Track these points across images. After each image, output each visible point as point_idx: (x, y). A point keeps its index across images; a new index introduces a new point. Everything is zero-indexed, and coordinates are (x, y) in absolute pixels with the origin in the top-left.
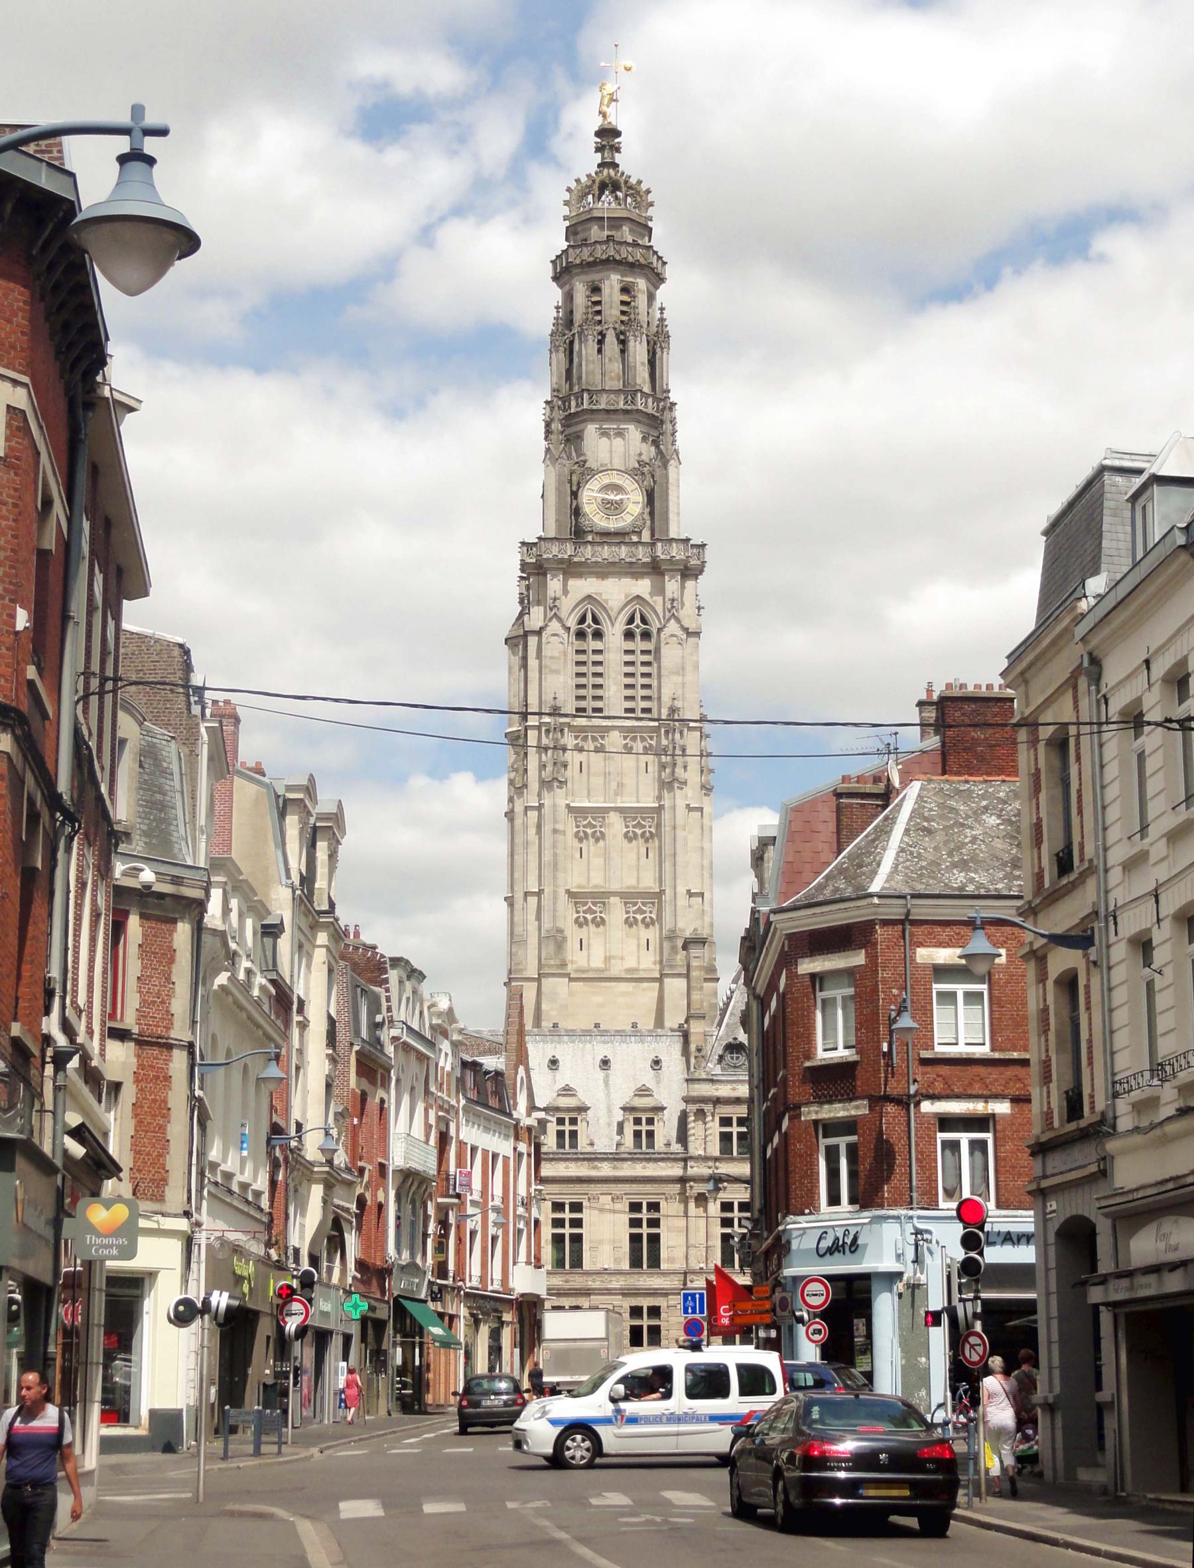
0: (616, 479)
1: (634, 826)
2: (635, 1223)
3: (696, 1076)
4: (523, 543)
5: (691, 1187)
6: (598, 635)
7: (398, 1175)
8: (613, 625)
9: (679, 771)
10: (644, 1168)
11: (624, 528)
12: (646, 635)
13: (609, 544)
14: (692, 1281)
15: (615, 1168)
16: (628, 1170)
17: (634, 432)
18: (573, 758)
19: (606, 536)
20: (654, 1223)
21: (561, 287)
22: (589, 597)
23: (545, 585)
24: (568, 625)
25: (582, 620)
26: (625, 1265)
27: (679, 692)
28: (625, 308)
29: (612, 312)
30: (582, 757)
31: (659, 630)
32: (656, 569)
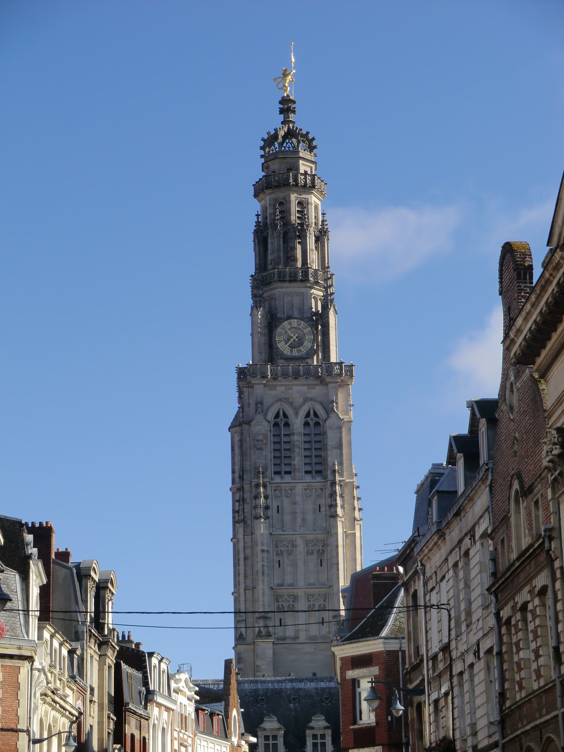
1: (312, 546)
6: (287, 424)
12: (317, 424)
21: (260, 201)
25: (277, 416)
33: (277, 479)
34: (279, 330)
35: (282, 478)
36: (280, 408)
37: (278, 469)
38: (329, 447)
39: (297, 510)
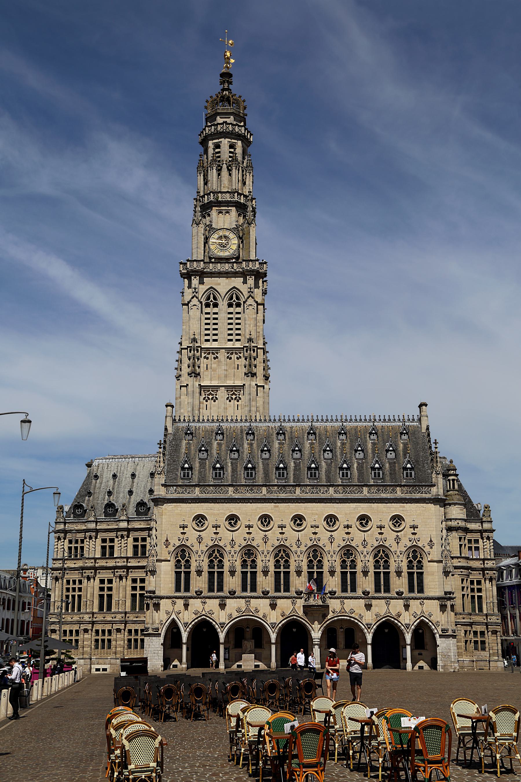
0: (227, 233)
6: (216, 305)
11: (228, 256)
13: (220, 263)
18: (203, 362)
19: (220, 260)
24: (202, 300)
25: (208, 298)
28: (231, 155)
31: (244, 302)
36: (210, 294)
37: (207, 338)
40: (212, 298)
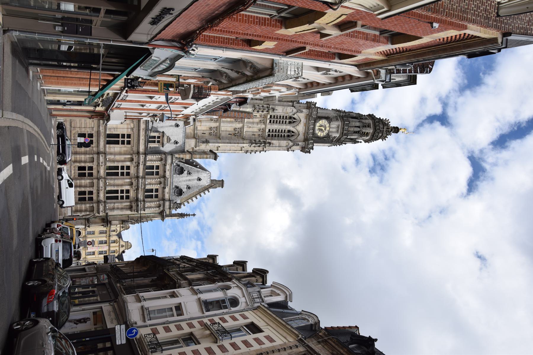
1: (238, 131)
2: (123, 136)
3: (174, 158)
4: (316, 103)
5: (136, 156)
6: (290, 123)
7: (268, 64)
8: (293, 127)
9: (254, 145)
10: (143, 139)
14: (102, 156)
15: (143, 129)
16: (142, 133)
17: (337, 135)
20: (123, 142)
22: (301, 121)
23: (304, 109)
24: (295, 115)
25: (294, 119)
26: (108, 132)
27: (274, 145)
29: (365, 130)
30: (258, 116)
31: (291, 140)
32: (306, 140)
33: (269, 117)
34: (326, 122)
35: (269, 119)
37: (272, 117)
38: (280, 141)
39: (254, 125)
40: (294, 120)
